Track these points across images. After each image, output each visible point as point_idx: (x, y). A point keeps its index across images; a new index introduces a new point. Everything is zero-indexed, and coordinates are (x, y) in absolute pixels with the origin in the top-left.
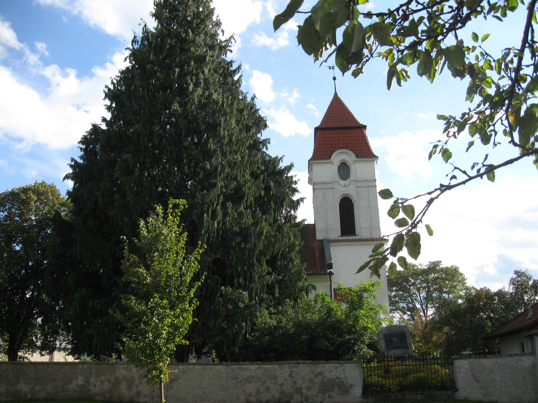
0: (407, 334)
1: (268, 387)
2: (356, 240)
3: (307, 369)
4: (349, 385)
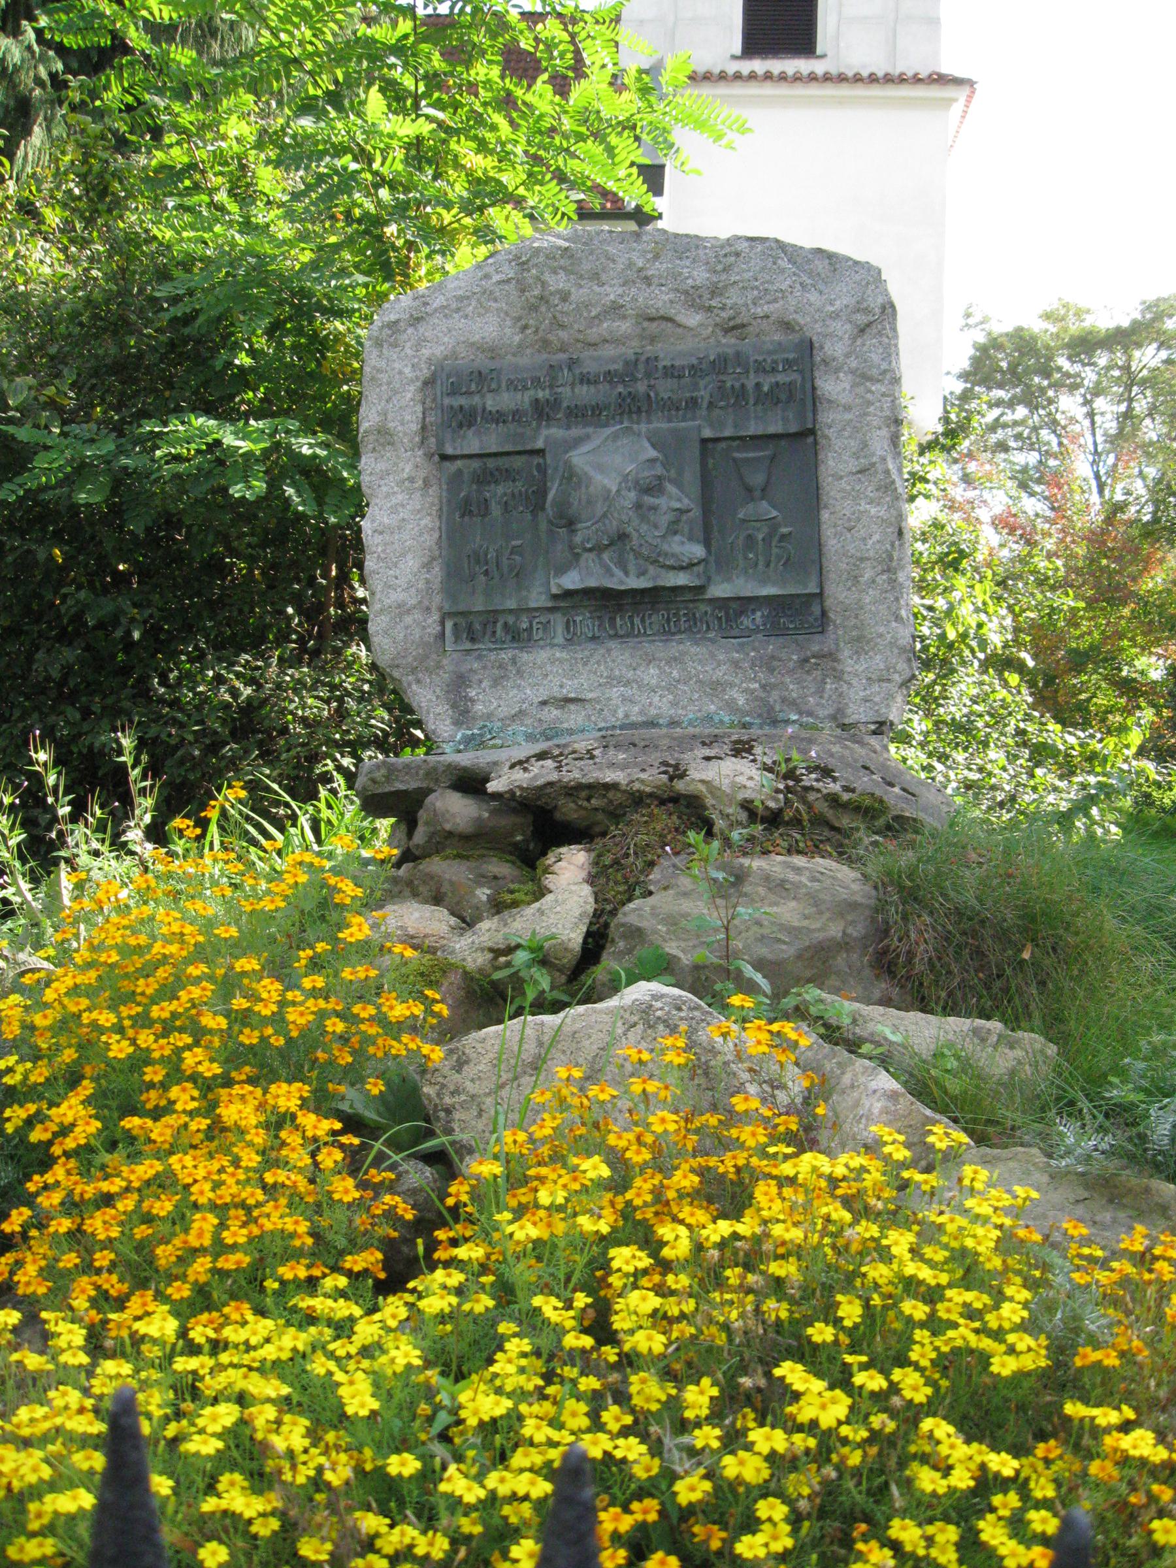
0: (832, 387)
2: (812, 78)
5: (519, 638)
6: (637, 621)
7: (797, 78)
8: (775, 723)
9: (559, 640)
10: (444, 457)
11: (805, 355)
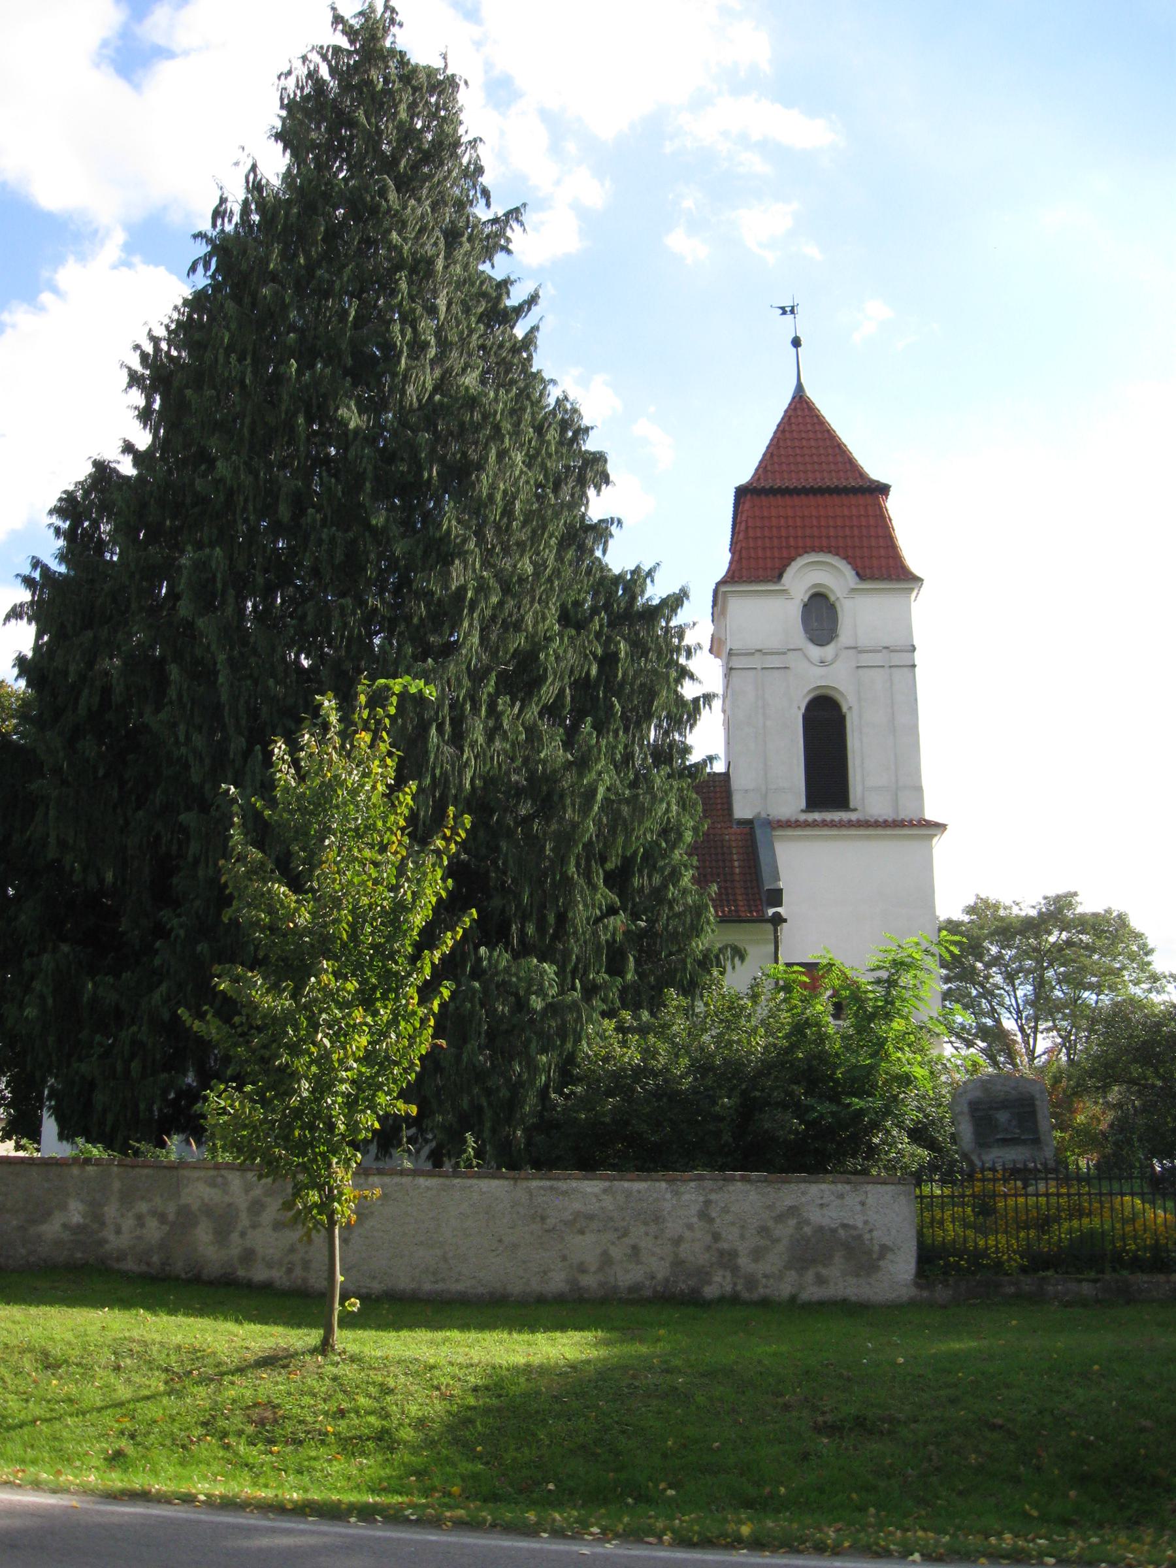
0: (1037, 1103)
1: (635, 1248)
2: (850, 824)
3: (753, 1196)
4: (876, 1248)
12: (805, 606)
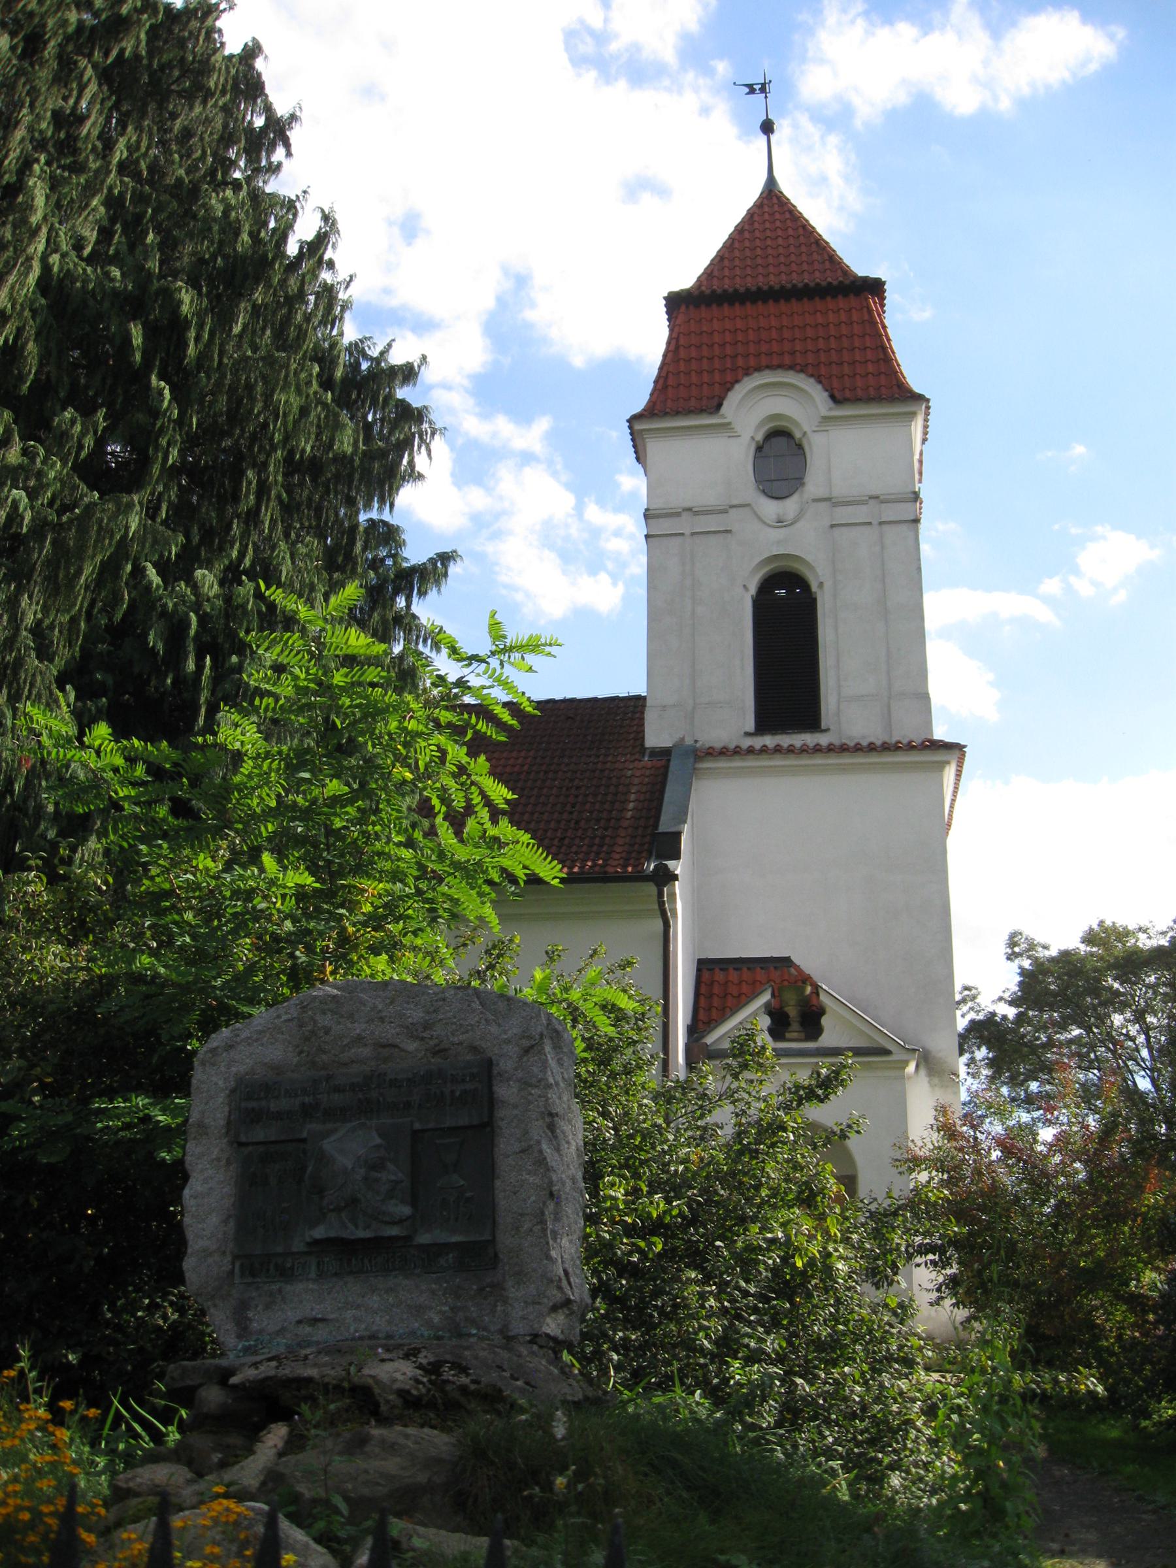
0: (505, 1091)
2: (817, 749)
5: (286, 1274)
6: (366, 1261)
7: (804, 750)
8: (460, 1335)
9: (313, 1275)
10: (241, 1144)
11: (486, 1070)
12: (759, 449)
